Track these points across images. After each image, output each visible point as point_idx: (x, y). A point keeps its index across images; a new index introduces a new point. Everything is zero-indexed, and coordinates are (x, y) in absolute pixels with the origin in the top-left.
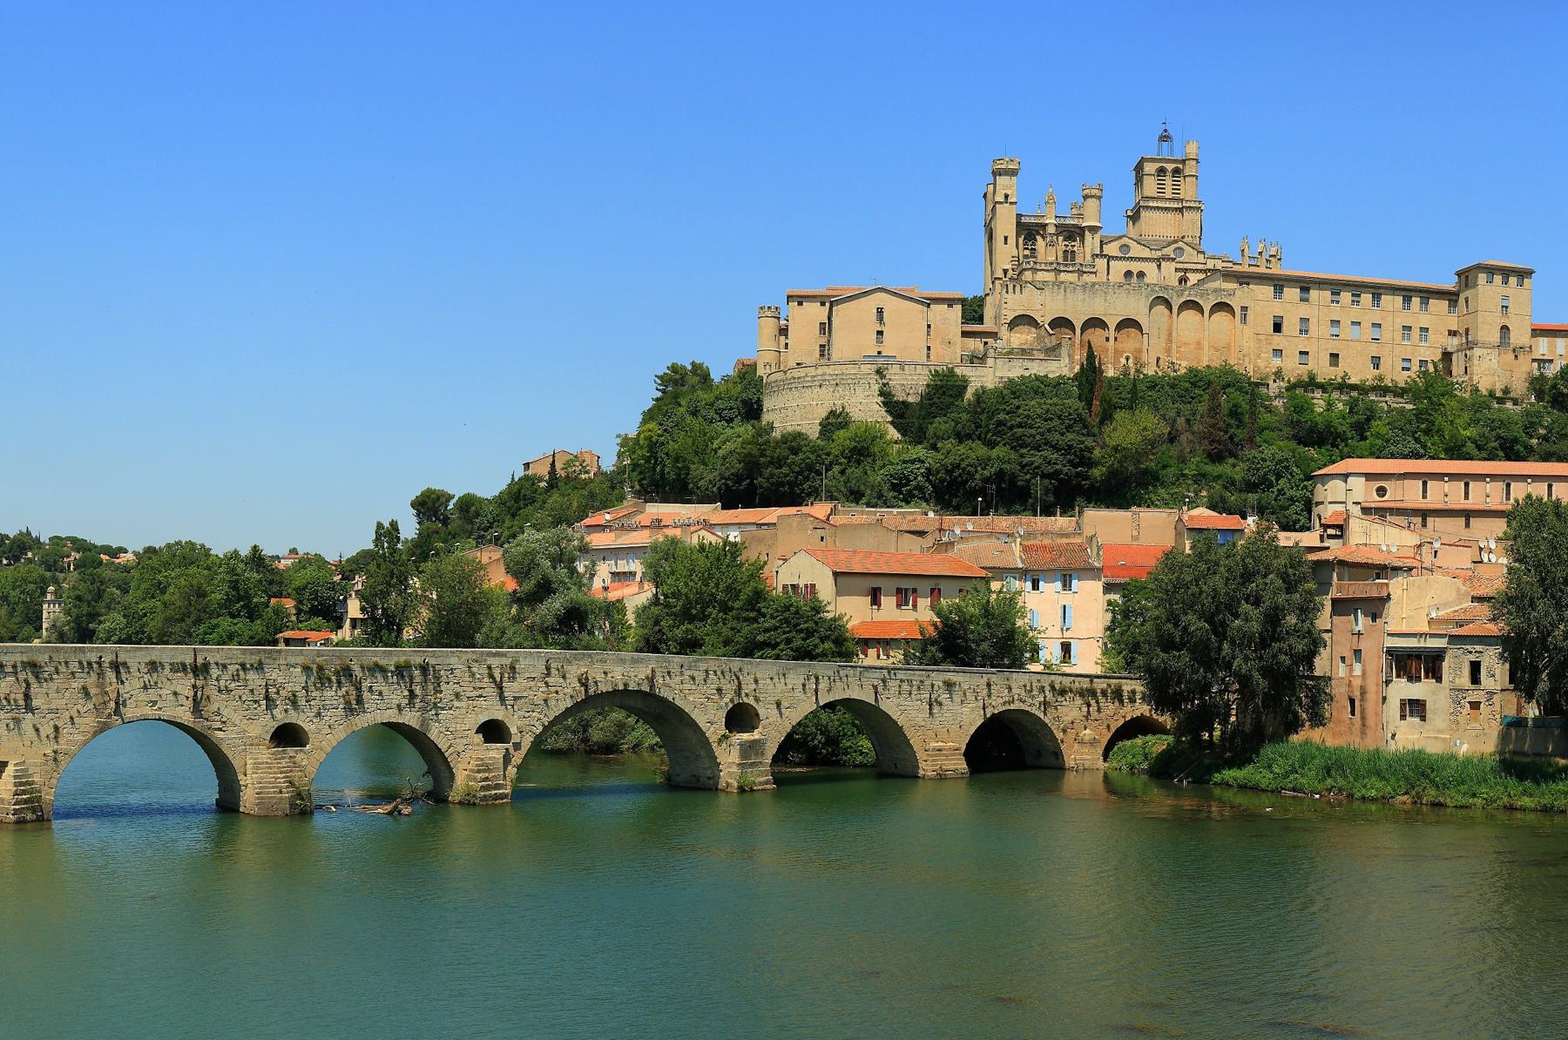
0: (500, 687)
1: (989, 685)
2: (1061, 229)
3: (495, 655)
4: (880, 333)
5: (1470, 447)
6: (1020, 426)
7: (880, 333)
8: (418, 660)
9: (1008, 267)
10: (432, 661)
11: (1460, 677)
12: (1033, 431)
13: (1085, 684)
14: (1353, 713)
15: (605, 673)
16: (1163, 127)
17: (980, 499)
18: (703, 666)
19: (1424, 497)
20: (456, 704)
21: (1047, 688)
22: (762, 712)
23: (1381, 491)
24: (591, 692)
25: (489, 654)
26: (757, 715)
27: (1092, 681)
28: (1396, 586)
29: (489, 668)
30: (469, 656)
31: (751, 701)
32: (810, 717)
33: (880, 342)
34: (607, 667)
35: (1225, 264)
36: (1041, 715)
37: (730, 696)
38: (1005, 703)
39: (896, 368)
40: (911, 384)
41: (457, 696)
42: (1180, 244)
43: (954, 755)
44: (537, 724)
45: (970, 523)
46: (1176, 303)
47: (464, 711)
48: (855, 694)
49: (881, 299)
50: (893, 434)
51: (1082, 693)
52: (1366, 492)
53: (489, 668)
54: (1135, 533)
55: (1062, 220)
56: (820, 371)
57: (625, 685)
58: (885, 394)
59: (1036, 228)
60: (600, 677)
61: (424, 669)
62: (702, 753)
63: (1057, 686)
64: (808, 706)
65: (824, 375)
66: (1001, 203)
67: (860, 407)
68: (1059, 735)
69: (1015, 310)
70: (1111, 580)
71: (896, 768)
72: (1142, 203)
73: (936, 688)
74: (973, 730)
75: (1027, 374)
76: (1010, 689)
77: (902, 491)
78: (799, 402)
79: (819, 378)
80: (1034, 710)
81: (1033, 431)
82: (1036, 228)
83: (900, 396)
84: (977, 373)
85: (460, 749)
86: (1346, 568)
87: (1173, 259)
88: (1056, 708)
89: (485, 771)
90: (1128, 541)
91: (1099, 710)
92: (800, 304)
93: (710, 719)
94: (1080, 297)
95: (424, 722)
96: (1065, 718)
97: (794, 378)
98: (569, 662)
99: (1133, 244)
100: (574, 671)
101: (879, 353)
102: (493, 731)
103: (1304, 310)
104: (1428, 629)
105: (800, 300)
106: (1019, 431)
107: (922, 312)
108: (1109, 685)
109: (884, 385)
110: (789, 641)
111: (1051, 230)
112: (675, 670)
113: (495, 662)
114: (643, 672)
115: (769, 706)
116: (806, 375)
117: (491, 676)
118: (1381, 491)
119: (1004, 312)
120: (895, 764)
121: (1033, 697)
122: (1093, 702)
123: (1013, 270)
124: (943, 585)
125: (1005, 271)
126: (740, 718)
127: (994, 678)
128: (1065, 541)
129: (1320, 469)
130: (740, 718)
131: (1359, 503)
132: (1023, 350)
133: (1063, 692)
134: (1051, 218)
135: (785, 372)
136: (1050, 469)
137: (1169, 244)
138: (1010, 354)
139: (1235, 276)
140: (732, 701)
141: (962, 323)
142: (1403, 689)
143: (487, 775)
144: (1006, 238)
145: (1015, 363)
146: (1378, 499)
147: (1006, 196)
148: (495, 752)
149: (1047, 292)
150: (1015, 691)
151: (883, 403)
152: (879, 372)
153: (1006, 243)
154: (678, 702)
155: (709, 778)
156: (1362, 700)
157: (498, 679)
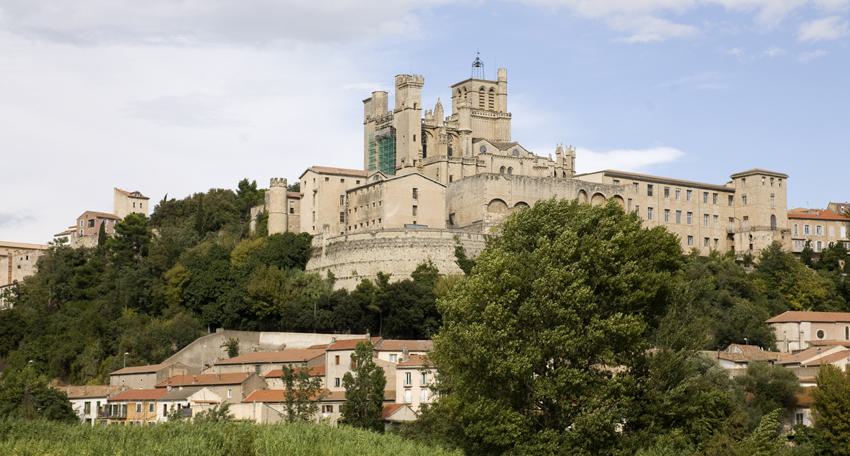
9: (417, 158)
16: (476, 55)
23: (821, 334)
58: (460, 253)
83: (469, 257)
94: (534, 188)
116: (397, 238)
118: (821, 334)
135: (373, 235)
144: (414, 140)
146: (818, 339)
152: (456, 238)
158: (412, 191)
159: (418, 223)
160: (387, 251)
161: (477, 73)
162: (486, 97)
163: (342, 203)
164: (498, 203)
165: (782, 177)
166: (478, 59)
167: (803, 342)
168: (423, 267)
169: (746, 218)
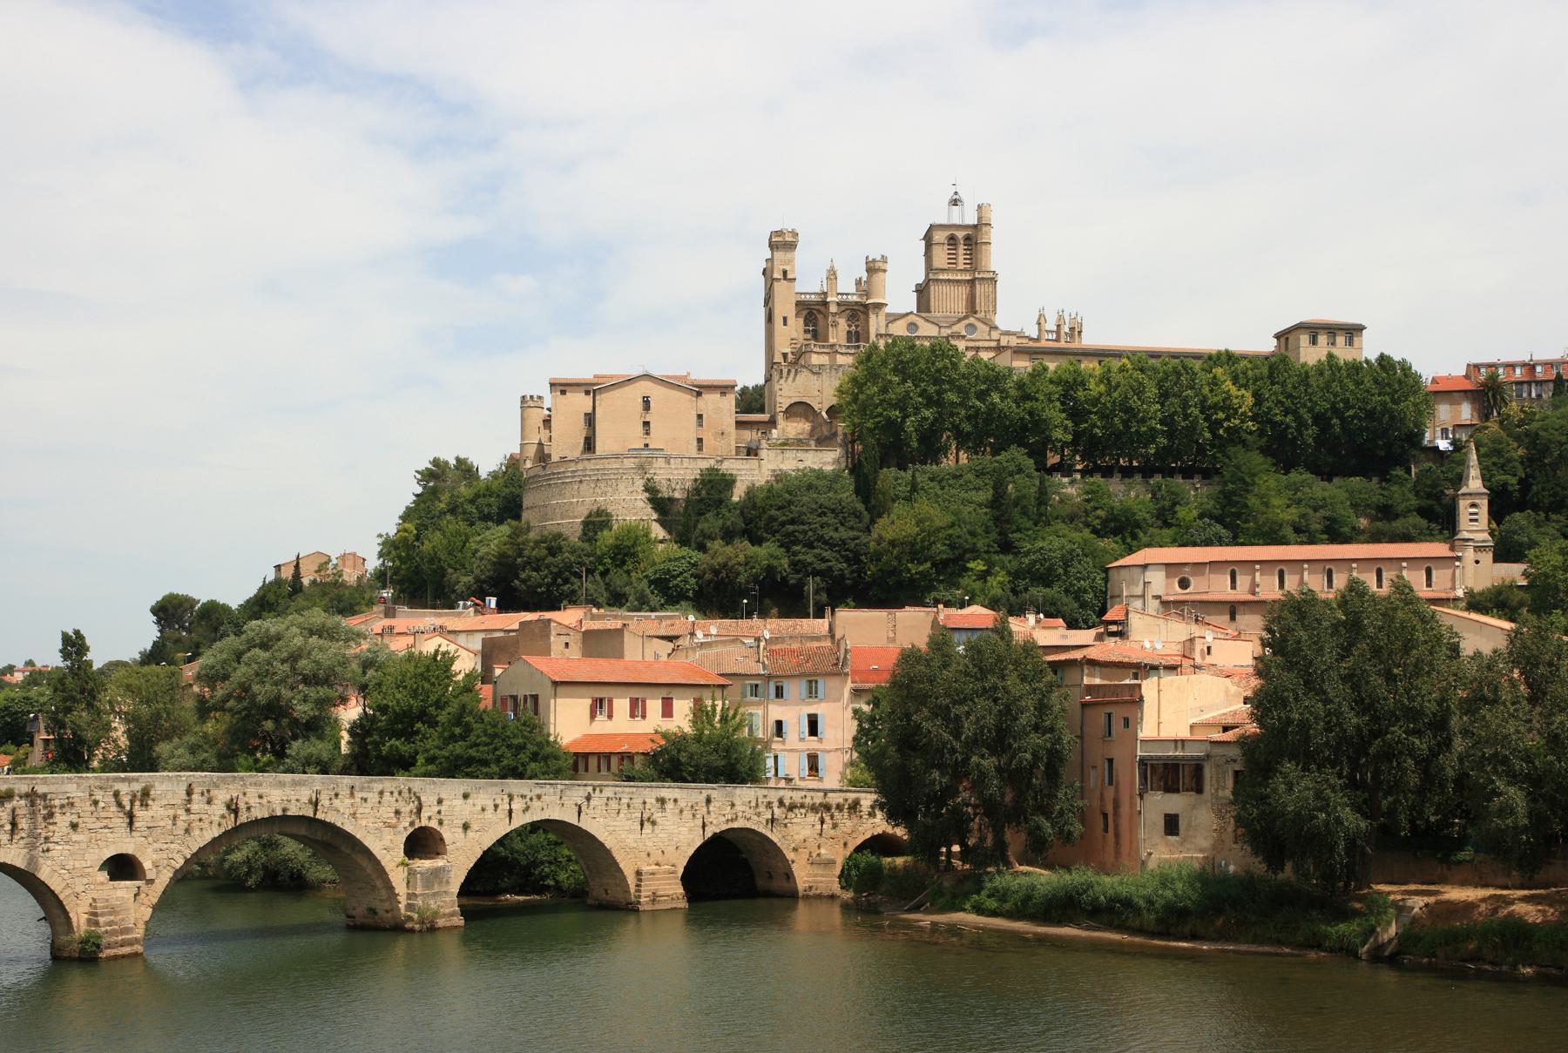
0: (131, 817)
1: (708, 801)
2: (843, 308)
3: (123, 780)
4: (646, 424)
5: (1288, 531)
6: (792, 522)
7: (646, 424)
8: (24, 788)
9: (788, 350)
10: (41, 789)
11: (1224, 788)
12: (806, 527)
13: (819, 798)
14: (1106, 830)
15: (260, 797)
17: (745, 601)
18: (377, 787)
19: (1233, 587)
20: (75, 837)
21: (776, 804)
22: (447, 836)
24: (243, 818)
25: (116, 780)
26: (442, 840)
27: (825, 795)
28: (1149, 687)
29: (116, 794)
30: (91, 782)
31: (434, 824)
32: (514, 834)
34: (262, 791)
35: (1020, 341)
36: (769, 834)
37: (409, 820)
38: (728, 820)
39: (661, 463)
40: (678, 477)
41: (74, 826)
42: (972, 320)
43: (669, 878)
44: (177, 857)
45: (715, 627)
47: (84, 846)
48: (555, 814)
49: (645, 388)
50: (658, 532)
51: (814, 808)
52: (1167, 585)
53: (116, 794)
54: (891, 635)
55: (845, 297)
56: (580, 466)
57: (284, 810)
58: (650, 489)
59: (817, 307)
60: (254, 801)
61: (32, 796)
62: (379, 883)
63: (787, 802)
64: (502, 828)
65: (585, 470)
66: (779, 280)
67: (624, 504)
68: (790, 856)
69: (790, 397)
70: (859, 685)
71: (607, 894)
72: (931, 276)
73: (648, 806)
74: (691, 851)
75: (801, 466)
76: (733, 805)
77: (667, 592)
79: (580, 473)
80: (762, 830)
81: (806, 527)
82: (817, 307)
83: (665, 493)
84: (747, 467)
85: (79, 889)
86: (1097, 668)
87: (964, 337)
88: (786, 826)
89: (110, 914)
90: (884, 643)
91: (835, 826)
92: (563, 392)
93: (387, 847)
95: (32, 860)
96: (796, 837)
97: (554, 474)
98: (217, 786)
99: (920, 322)
100: (222, 796)
101: (647, 445)
102: (122, 867)
104: (1189, 735)
105: (563, 388)
106: (791, 528)
107: (690, 401)
108: (846, 800)
109: (648, 480)
110: (498, 761)
111: (833, 309)
112: (345, 792)
113: (124, 788)
114: (305, 794)
115: (457, 830)
117: (120, 805)
118: (1184, 584)
119: (779, 399)
120: (606, 891)
121: (759, 814)
122: (827, 819)
123: (792, 353)
124: (674, 693)
125: (785, 355)
126: (422, 843)
127: (714, 794)
128: (815, 644)
129: (1117, 559)
130: (422, 843)
131: (1160, 597)
132: (800, 440)
133: (792, 808)
134: (832, 296)
136: (824, 566)
137: (960, 320)
138: (785, 444)
139: (1027, 353)
140: (412, 824)
141: (737, 412)
142: (1159, 804)
143: (112, 918)
144: (785, 319)
145: (788, 454)
147: (785, 273)
148: (125, 888)
149: (825, 376)
150: (739, 808)
151: (648, 499)
153: (785, 324)
154: (348, 828)
155: (387, 912)
156: (1116, 814)
157: (128, 808)
158: (640, 400)
159: (650, 447)
161: (958, 217)
162: (961, 249)
164: (800, 409)
166: (956, 193)
167: (1149, 597)
168: (599, 513)
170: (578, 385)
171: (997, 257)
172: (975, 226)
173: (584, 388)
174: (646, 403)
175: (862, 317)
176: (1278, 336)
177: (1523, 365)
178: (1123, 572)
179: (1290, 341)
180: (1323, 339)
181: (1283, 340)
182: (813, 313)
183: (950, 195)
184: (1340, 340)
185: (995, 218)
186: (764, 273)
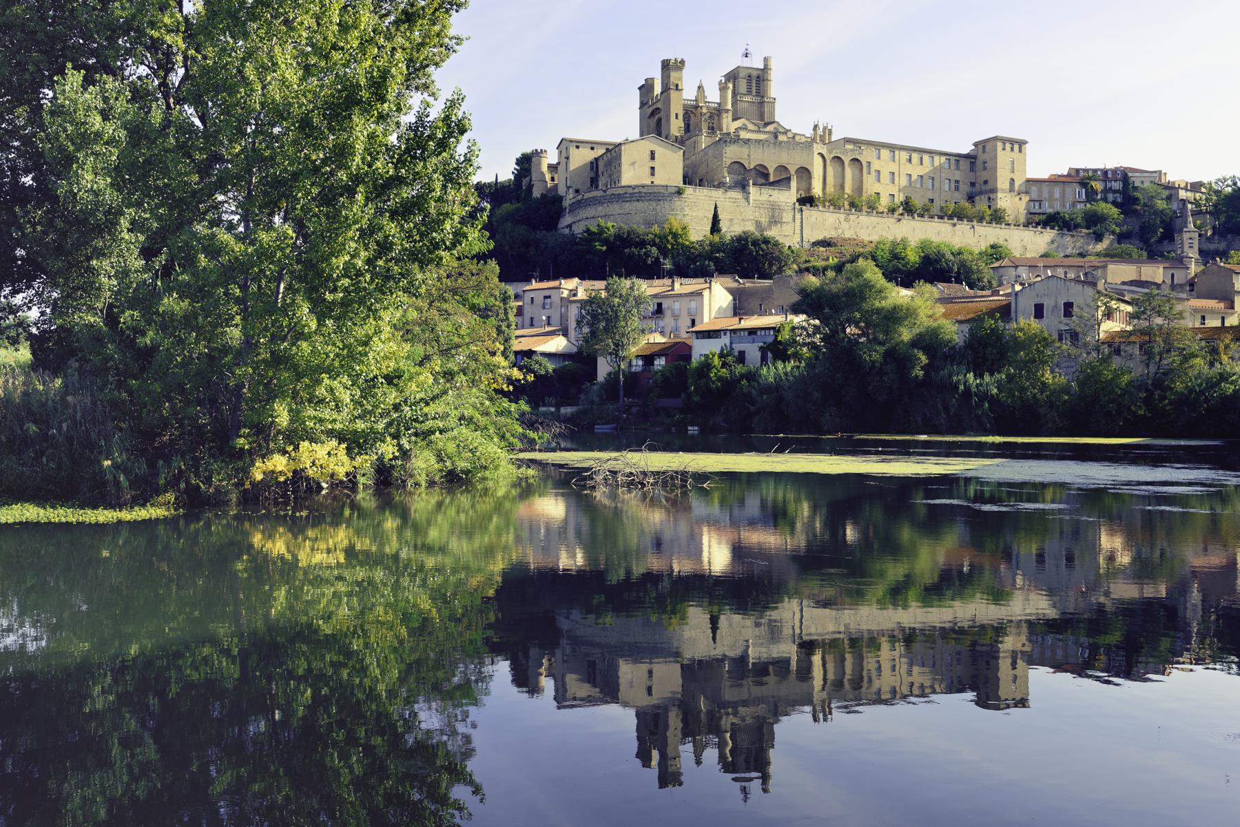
4: (653, 168)
7: (653, 168)
33: (653, 174)
46: (828, 157)
78: (620, 212)
92: (578, 147)
103: (893, 167)
144: (677, 115)
147: (677, 85)
160: (616, 206)
161: (747, 63)
162: (754, 85)
163: (592, 169)
164: (736, 166)
165: (1022, 143)
169: (986, 182)
170: (587, 142)
171: (775, 89)
172: (763, 70)
173: (590, 145)
174: (653, 156)
175: (716, 117)
176: (976, 144)
177: (1101, 170)
178: (1001, 270)
179: (987, 149)
180: (1008, 146)
181: (980, 147)
182: (690, 112)
183: (743, 51)
184: (1016, 147)
185: (773, 64)
186: (646, 88)
